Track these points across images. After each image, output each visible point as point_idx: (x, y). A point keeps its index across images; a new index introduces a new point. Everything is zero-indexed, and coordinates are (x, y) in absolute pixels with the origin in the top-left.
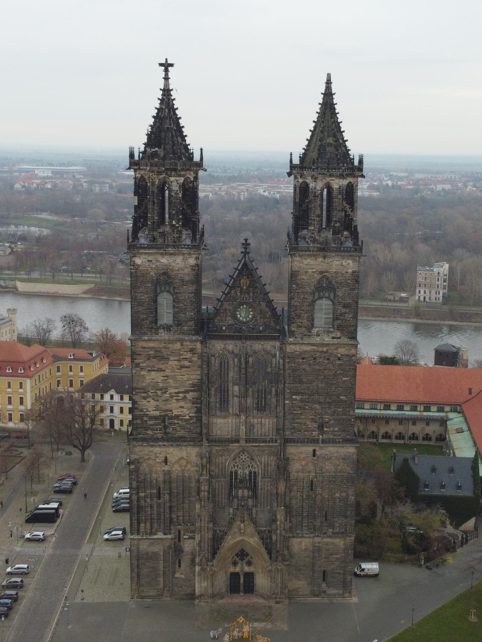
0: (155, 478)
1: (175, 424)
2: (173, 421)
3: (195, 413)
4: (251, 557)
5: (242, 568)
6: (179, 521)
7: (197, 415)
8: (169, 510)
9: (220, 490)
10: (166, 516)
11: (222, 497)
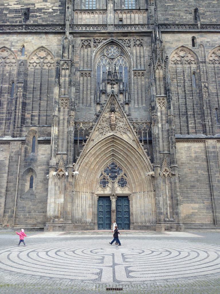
0: (9, 71)
1: (36, 16)
2: (35, 14)
3: (59, 6)
4: (125, 175)
5: (113, 189)
6: (33, 122)
7: (61, 8)
8: (22, 107)
9: (85, 85)
10: (17, 114)
11: (87, 93)
